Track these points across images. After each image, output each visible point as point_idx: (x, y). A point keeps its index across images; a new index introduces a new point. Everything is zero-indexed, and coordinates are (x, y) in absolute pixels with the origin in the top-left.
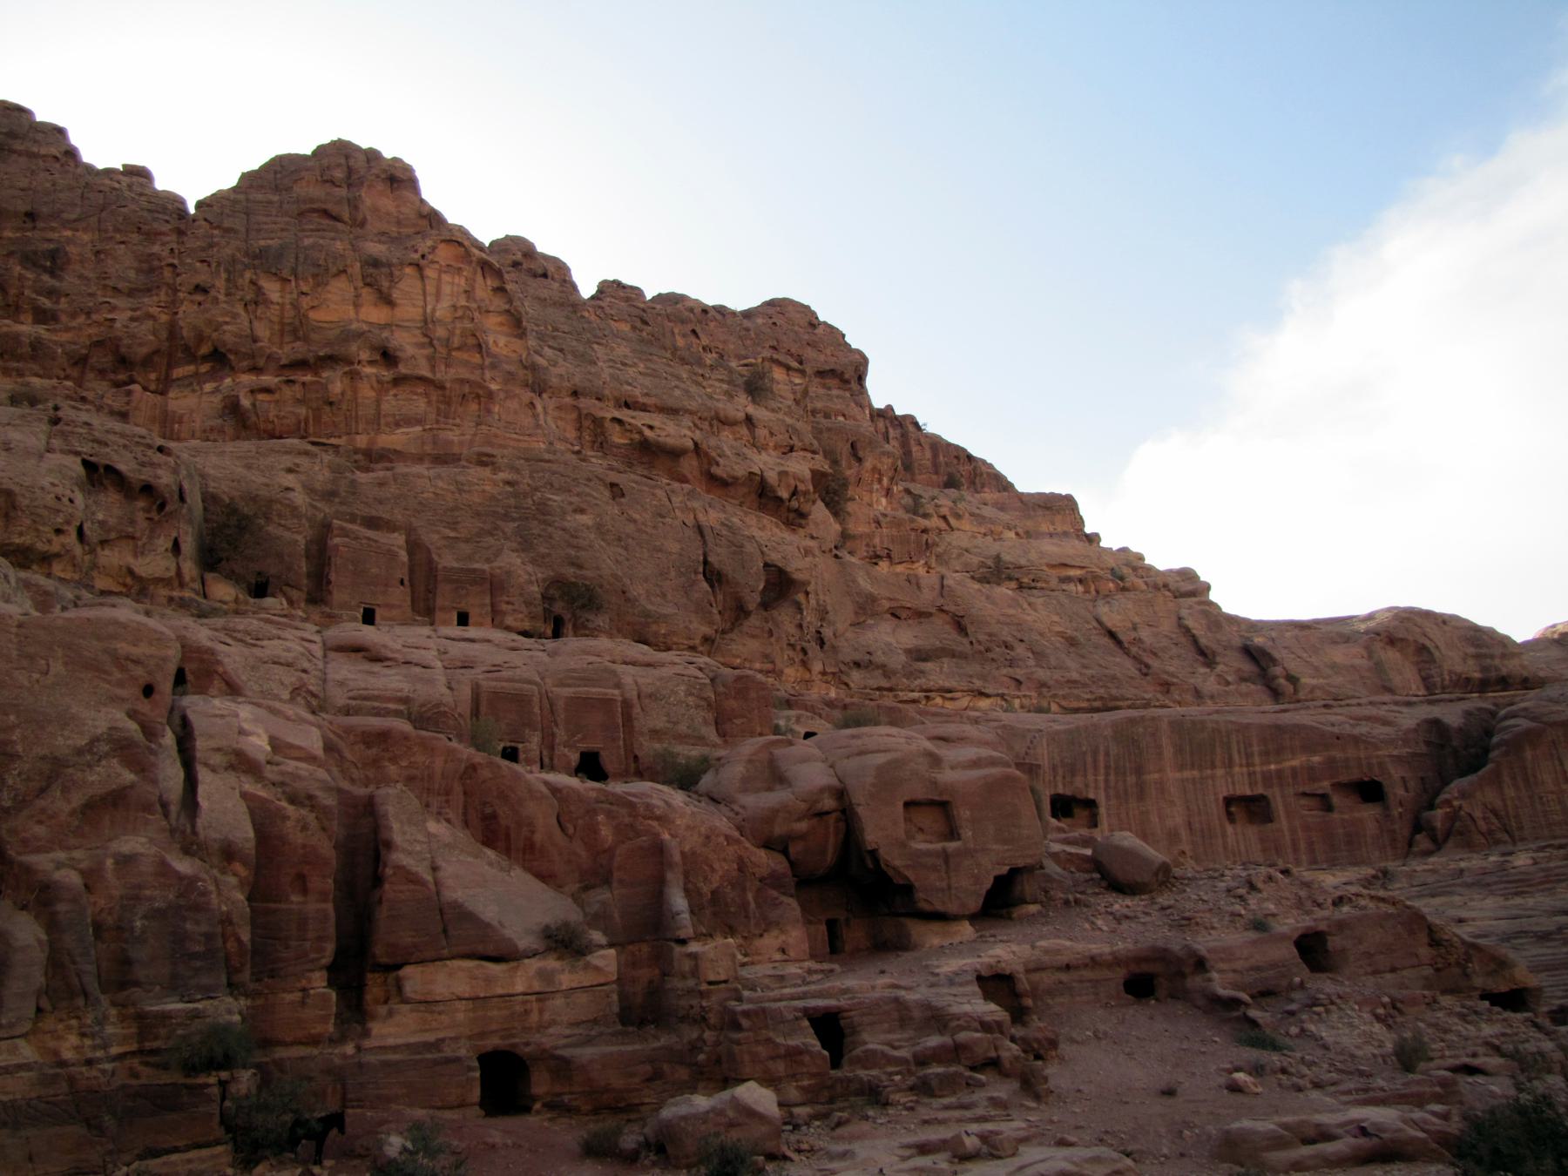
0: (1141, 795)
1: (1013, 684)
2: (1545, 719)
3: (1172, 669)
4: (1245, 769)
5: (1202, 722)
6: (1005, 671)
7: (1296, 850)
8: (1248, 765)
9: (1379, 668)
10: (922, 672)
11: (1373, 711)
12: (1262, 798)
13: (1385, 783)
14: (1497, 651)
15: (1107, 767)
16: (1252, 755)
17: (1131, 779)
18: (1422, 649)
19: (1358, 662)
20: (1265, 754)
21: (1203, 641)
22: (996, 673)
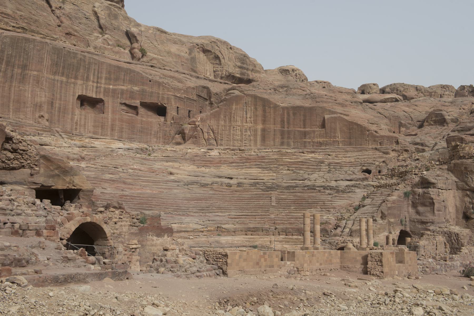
0: (23, 79)
2: (246, 92)
3: (77, 28)
4: (95, 84)
5: (77, 54)
7: (112, 130)
8: (97, 82)
9: (193, 60)
11: (176, 75)
12: (101, 101)
13: (168, 108)
14: (251, 68)
16: (101, 78)
17: (17, 71)
18: (217, 58)
19: (183, 54)
20: (108, 79)
21: (102, 21)
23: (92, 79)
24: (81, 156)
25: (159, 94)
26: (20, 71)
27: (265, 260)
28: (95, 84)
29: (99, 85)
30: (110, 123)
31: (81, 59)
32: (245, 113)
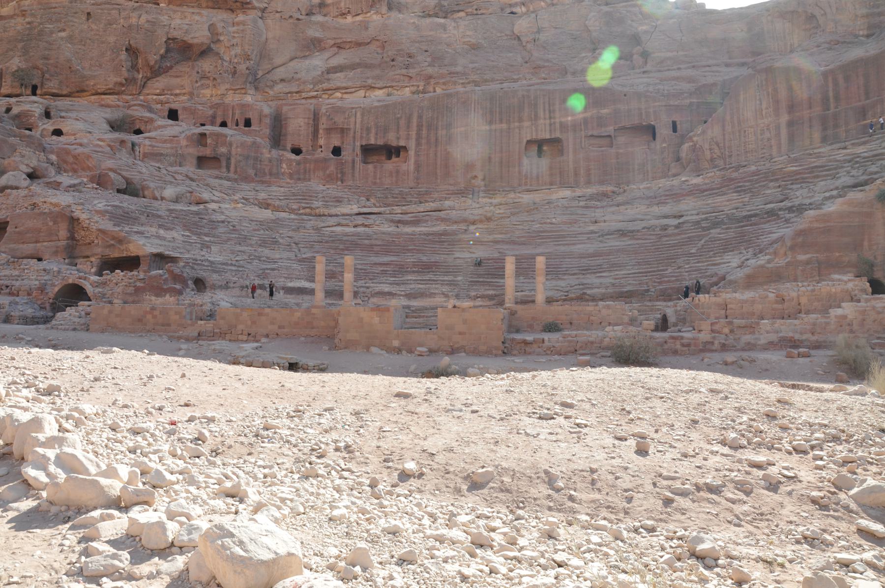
1: (407, 79)
3: (550, 56)
6: (399, 72)
8: (550, 118)
10: (329, 80)
15: (420, 127)
16: (554, 111)
22: (391, 73)
23: (542, 116)
24: (485, 216)
25: (640, 109)
26: (444, 132)
27: (155, 317)
28: (548, 122)
29: (552, 120)
30: (571, 166)
31: (523, 96)
32: (758, 102)
